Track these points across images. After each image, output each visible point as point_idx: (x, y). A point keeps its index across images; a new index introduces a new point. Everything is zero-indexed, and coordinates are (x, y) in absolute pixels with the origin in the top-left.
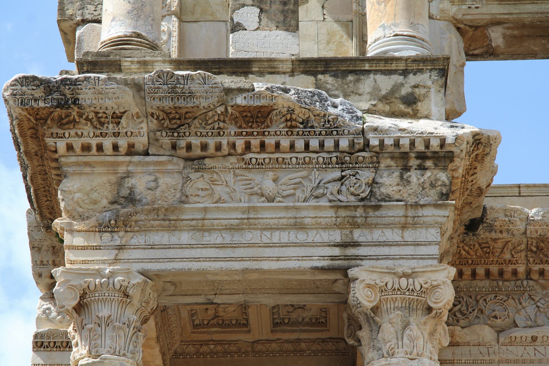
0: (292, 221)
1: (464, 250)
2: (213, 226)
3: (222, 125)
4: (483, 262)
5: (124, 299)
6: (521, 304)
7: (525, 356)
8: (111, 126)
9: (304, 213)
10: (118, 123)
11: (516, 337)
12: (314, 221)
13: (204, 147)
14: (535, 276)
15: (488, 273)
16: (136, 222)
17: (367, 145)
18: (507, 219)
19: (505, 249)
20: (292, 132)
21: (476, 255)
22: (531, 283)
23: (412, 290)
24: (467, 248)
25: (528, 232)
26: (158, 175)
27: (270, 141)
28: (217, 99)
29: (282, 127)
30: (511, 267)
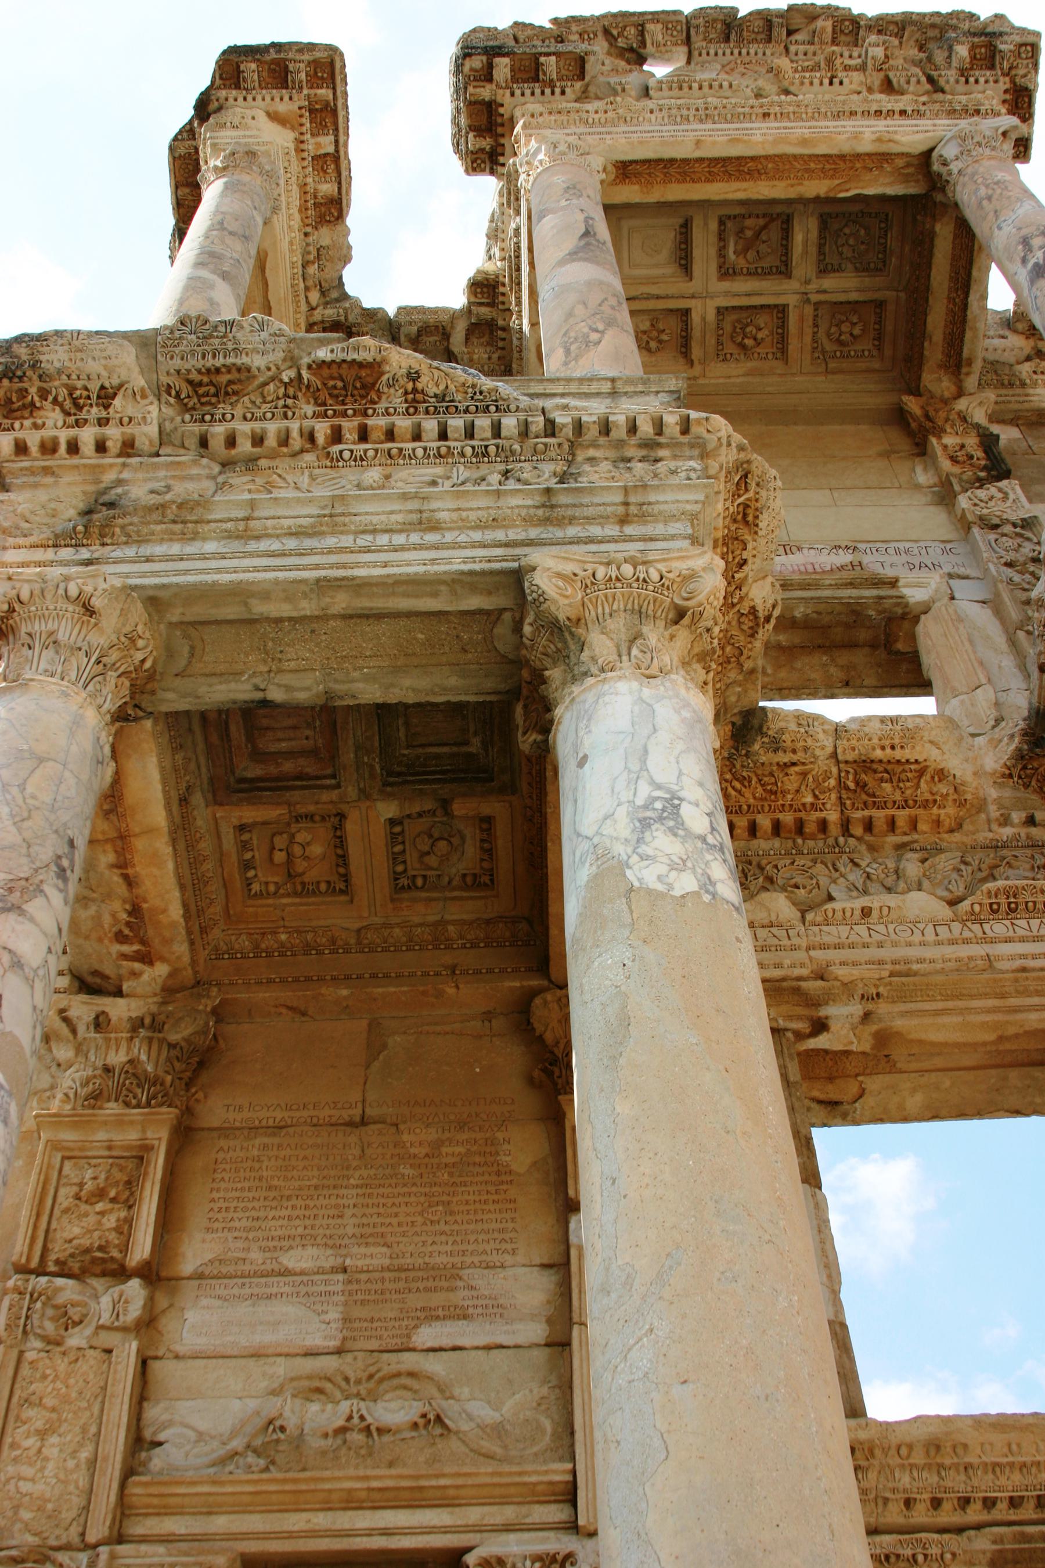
0: (415, 517)
1: (733, 788)
2: (266, 529)
3: (290, 402)
4: (766, 809)
5: (85, 618)
6: (836, 870)
7: (853, 938)
8: (95, 410)
9: (435, 505)
10: (106, 407)
11: (834, 911)
12: (455, 516)
13: (258, 440)
14: (858, 831)
15: (777, 828)
16: (123, 527)
17: (551, 428)
18: (802, 730)
19: (803, 788)
20: (416, 409)
21: (755, 798)
22: (852, 841)
23: (644, 580)
24: (738, 785)
25: (839, 751)
26: (171, 482)
27: (377, 423)
28: (282, 355)
29: (397, 401)
30: (816, 815)
